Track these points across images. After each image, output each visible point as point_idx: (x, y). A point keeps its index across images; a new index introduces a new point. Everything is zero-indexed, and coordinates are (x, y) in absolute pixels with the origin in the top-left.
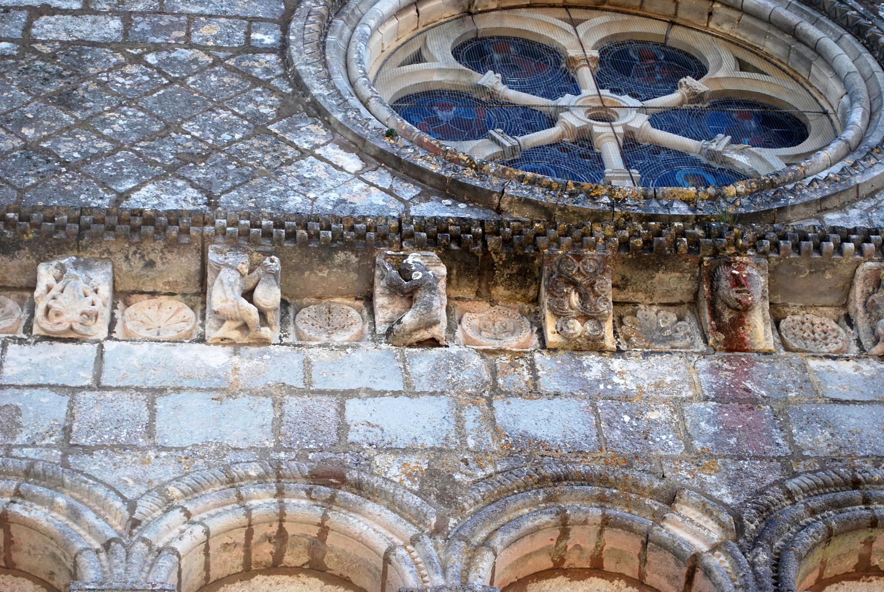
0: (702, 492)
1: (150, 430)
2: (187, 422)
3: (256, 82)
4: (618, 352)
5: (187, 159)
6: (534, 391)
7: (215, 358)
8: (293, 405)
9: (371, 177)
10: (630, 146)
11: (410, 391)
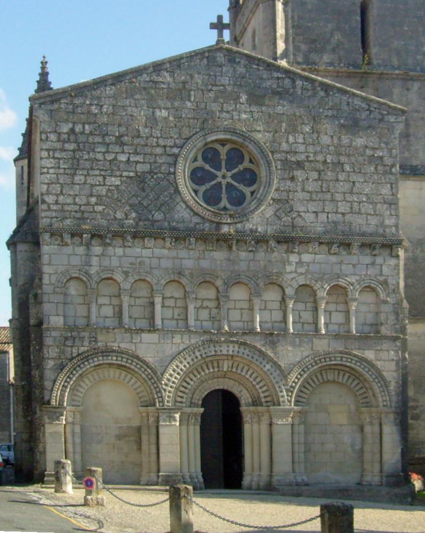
0: (221, 277)
1: (159, 266)
2: (165, 263)
3: (171, 184)
4: (216, 251)
5: (162, 205)
6: (204, 259)
7: (166, 252)
8: (176, 260)
9: (187, 210)
10: (229, 185)
11: (189, 258)
